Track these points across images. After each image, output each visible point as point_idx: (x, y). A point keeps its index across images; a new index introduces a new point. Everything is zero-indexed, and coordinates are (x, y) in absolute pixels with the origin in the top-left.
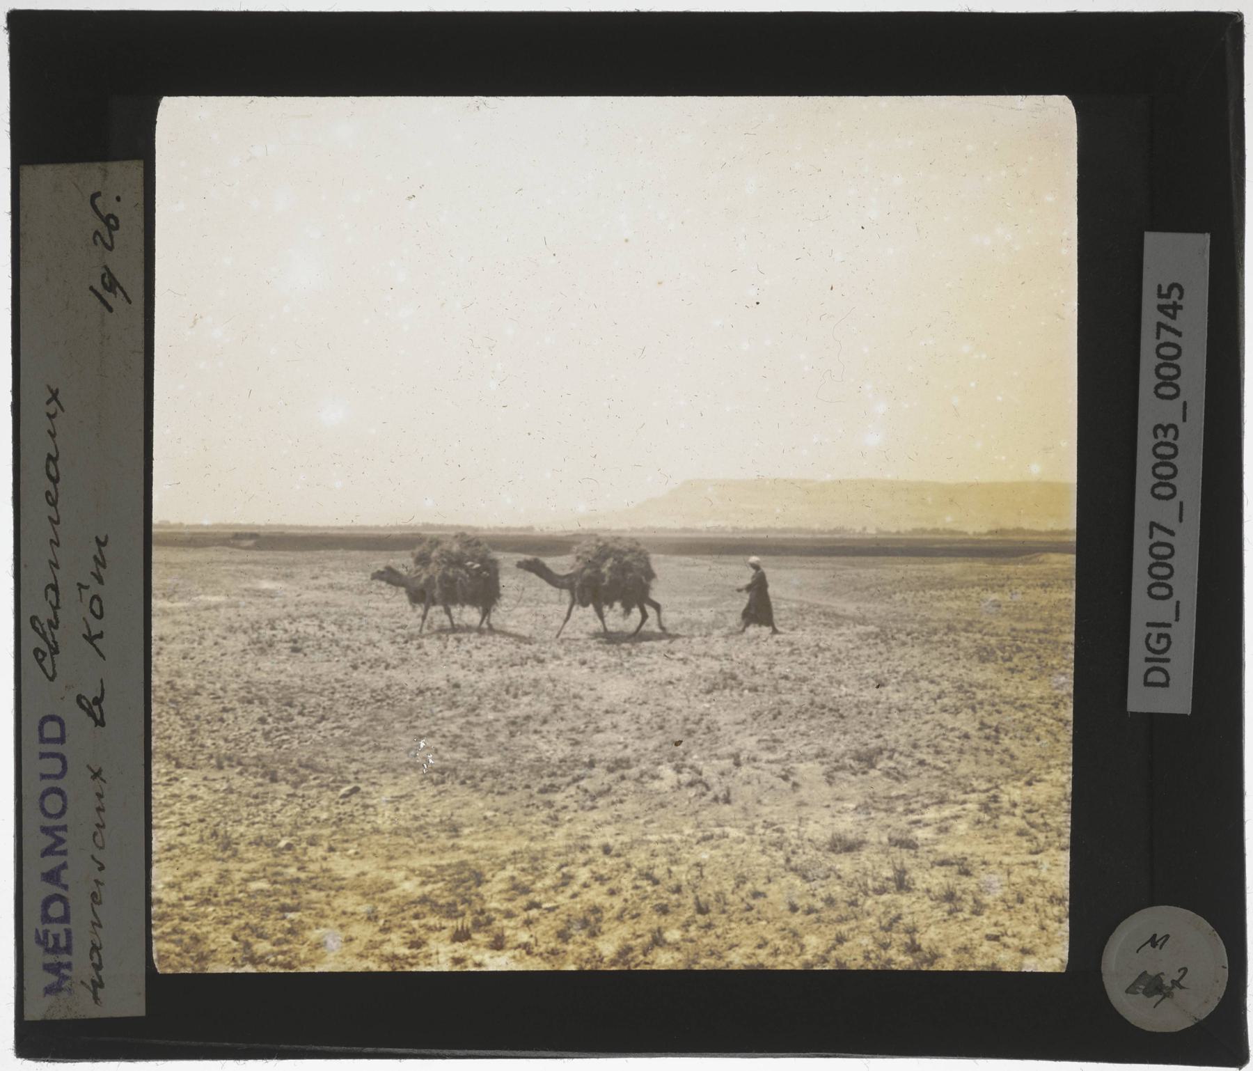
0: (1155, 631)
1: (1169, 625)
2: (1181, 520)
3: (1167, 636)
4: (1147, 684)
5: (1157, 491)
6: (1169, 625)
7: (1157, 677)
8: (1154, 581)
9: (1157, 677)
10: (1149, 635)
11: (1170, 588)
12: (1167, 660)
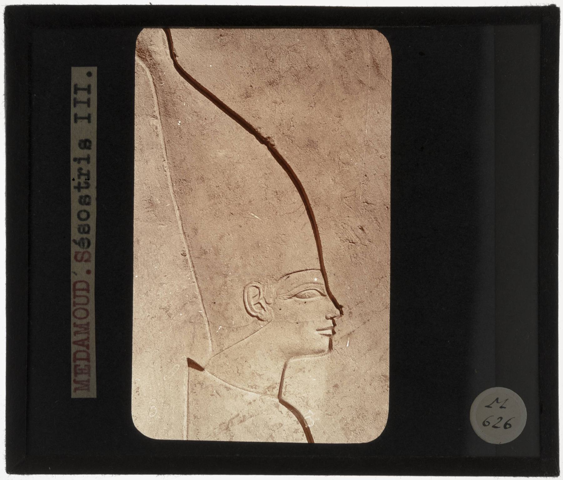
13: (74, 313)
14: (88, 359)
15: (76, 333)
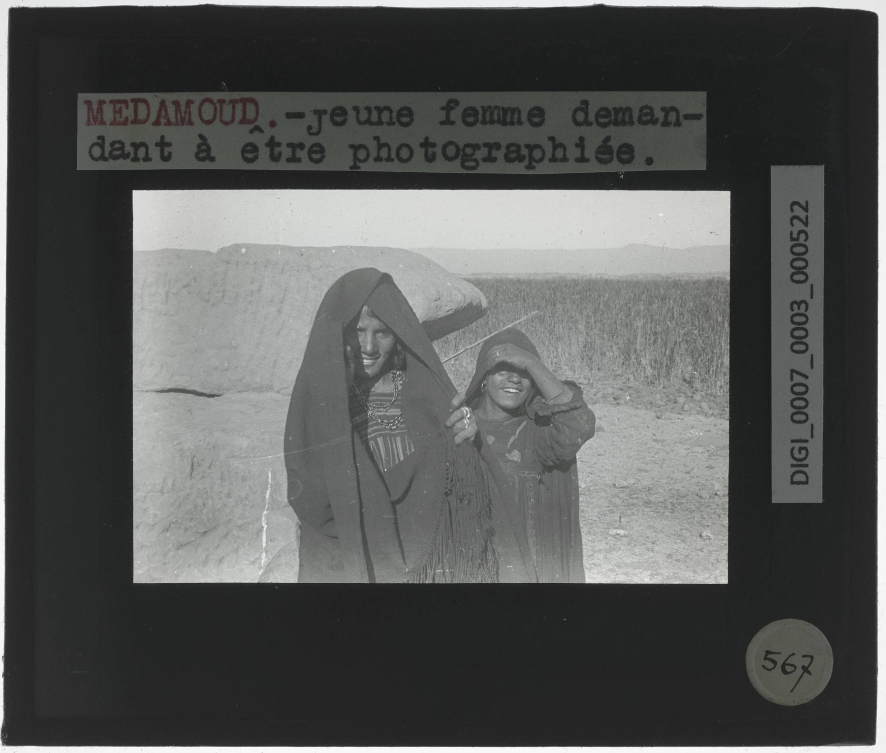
0: (797, 445)
1: (806, 441)
2: (812, 367)
3: (805, 449)
4: (793, 483)
5: (796, 347)
6: (806, 441)
7: (800, 477)
8: (795, 410)
9: (800, 477)
10: (793, 449)
11: (807, 415)
12: (806, 466)
13: (207, 100)
14: (136, 121)
15: (176, 104)
